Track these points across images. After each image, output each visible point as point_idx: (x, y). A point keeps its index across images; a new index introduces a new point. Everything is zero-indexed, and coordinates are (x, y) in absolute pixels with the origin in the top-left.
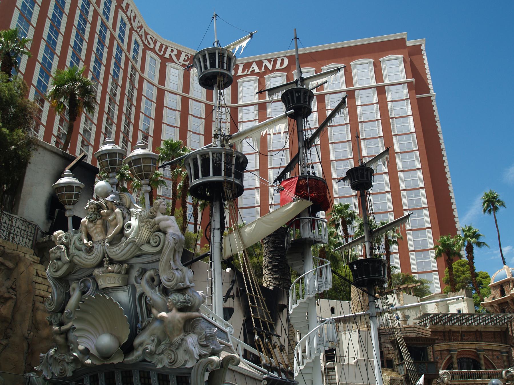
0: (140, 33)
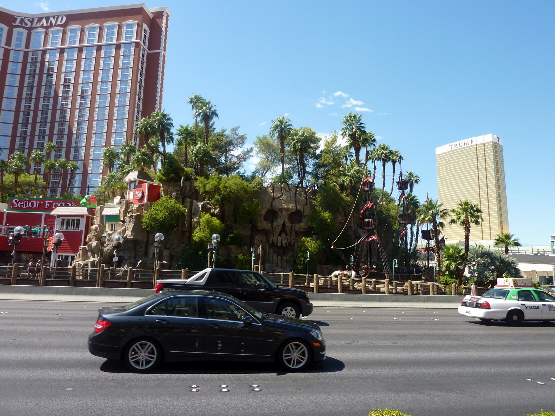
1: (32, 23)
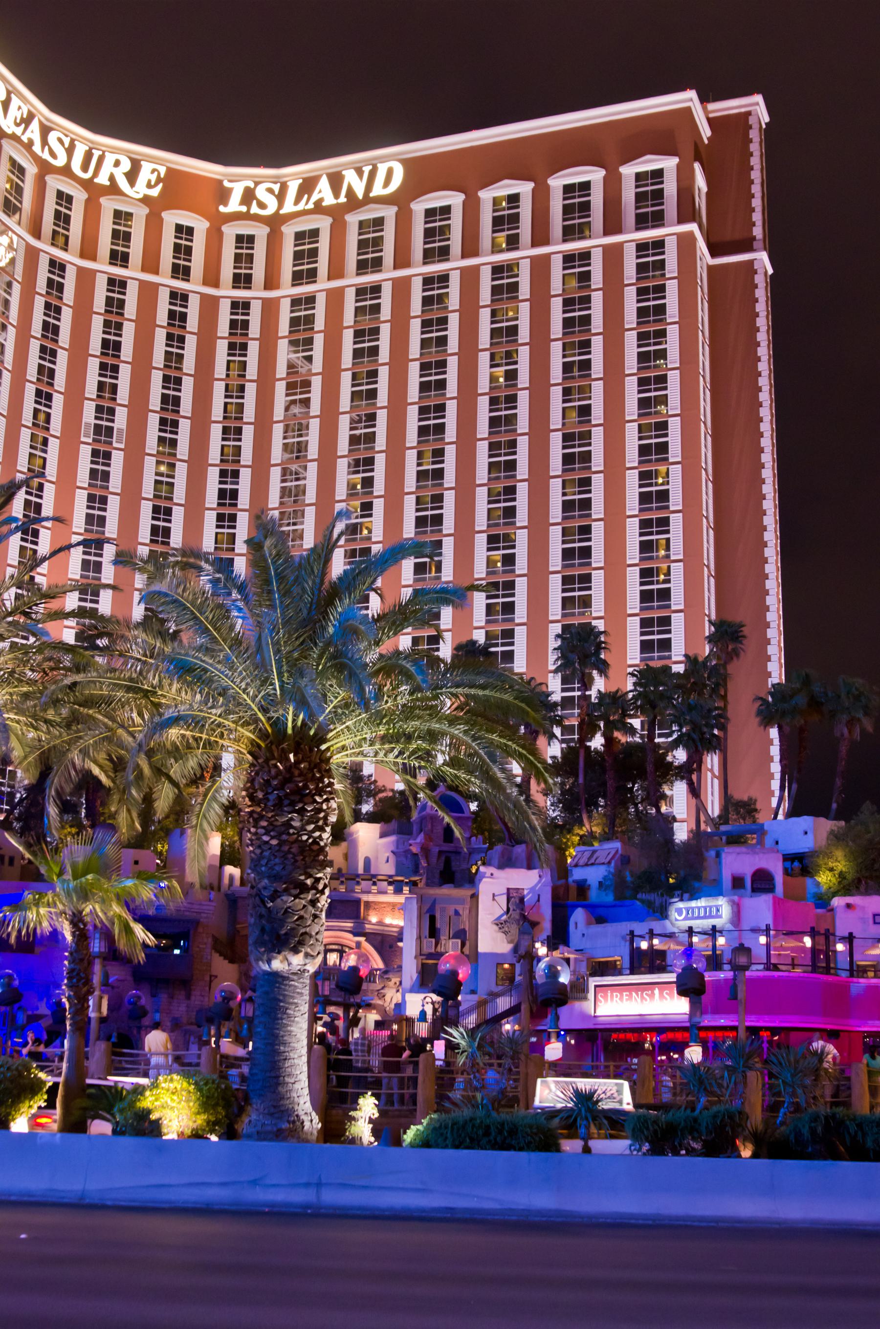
0: (25, 139)
1: (281, 198)
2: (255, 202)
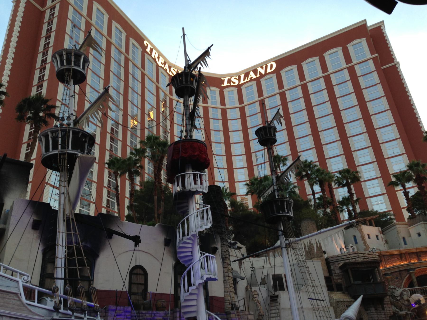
0: (165, 68)
1: (239, 80)
2: (232, 82)
